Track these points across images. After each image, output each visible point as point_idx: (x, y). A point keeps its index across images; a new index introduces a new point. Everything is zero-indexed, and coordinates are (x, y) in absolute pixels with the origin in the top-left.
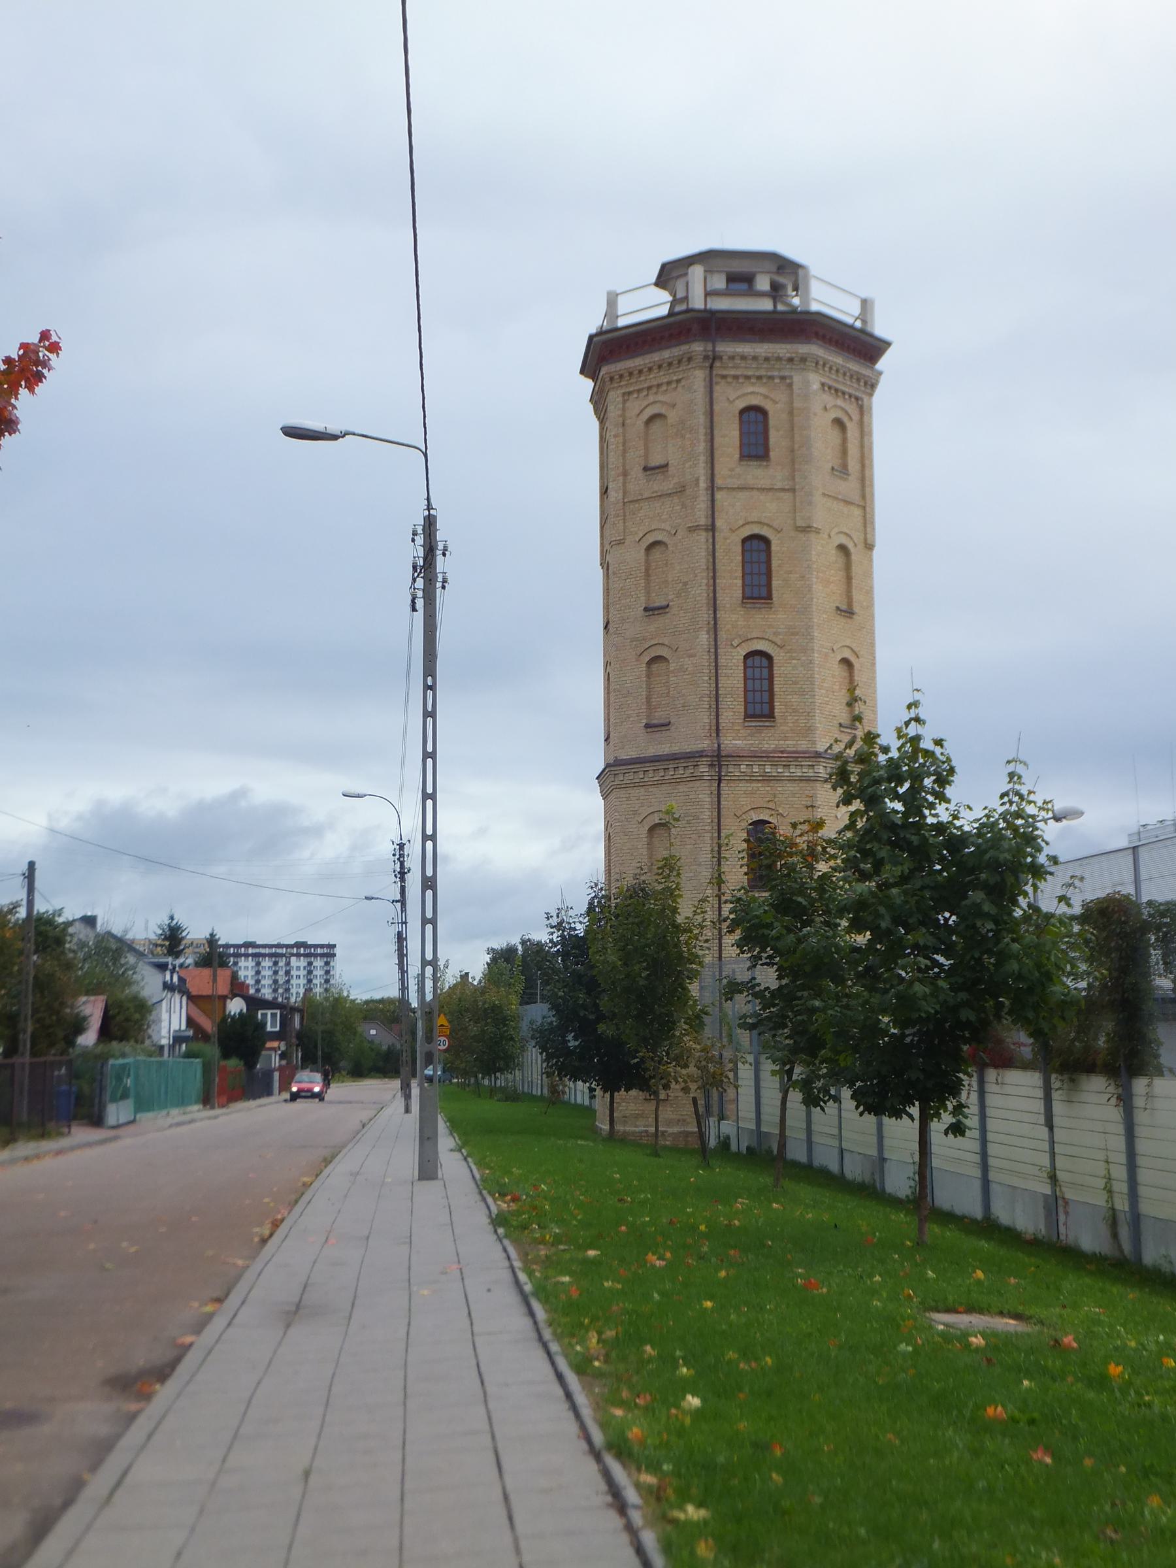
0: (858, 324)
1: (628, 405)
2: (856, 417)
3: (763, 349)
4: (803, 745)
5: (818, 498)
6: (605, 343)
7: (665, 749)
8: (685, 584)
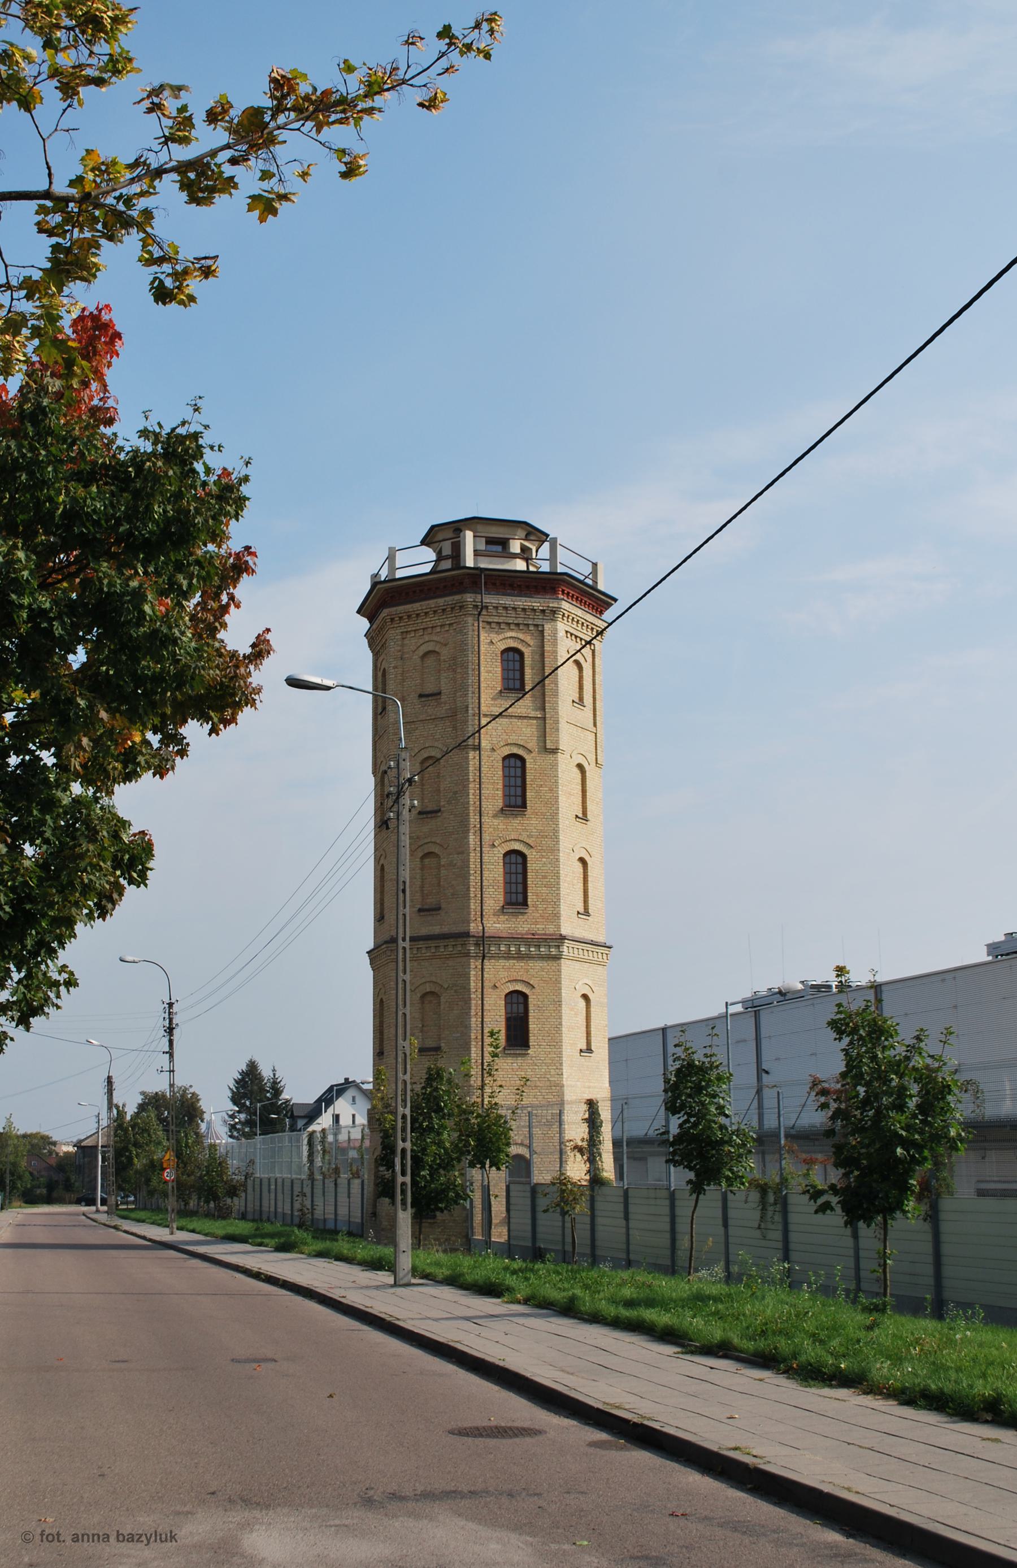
0: (589, 582)
1: (406, 642)
2: (590, 659)
3: (522, 602)
4: (551, 929)
5: (563, 726)
6: (386, 590)
7: (436, 930)
8: (455, 793)
